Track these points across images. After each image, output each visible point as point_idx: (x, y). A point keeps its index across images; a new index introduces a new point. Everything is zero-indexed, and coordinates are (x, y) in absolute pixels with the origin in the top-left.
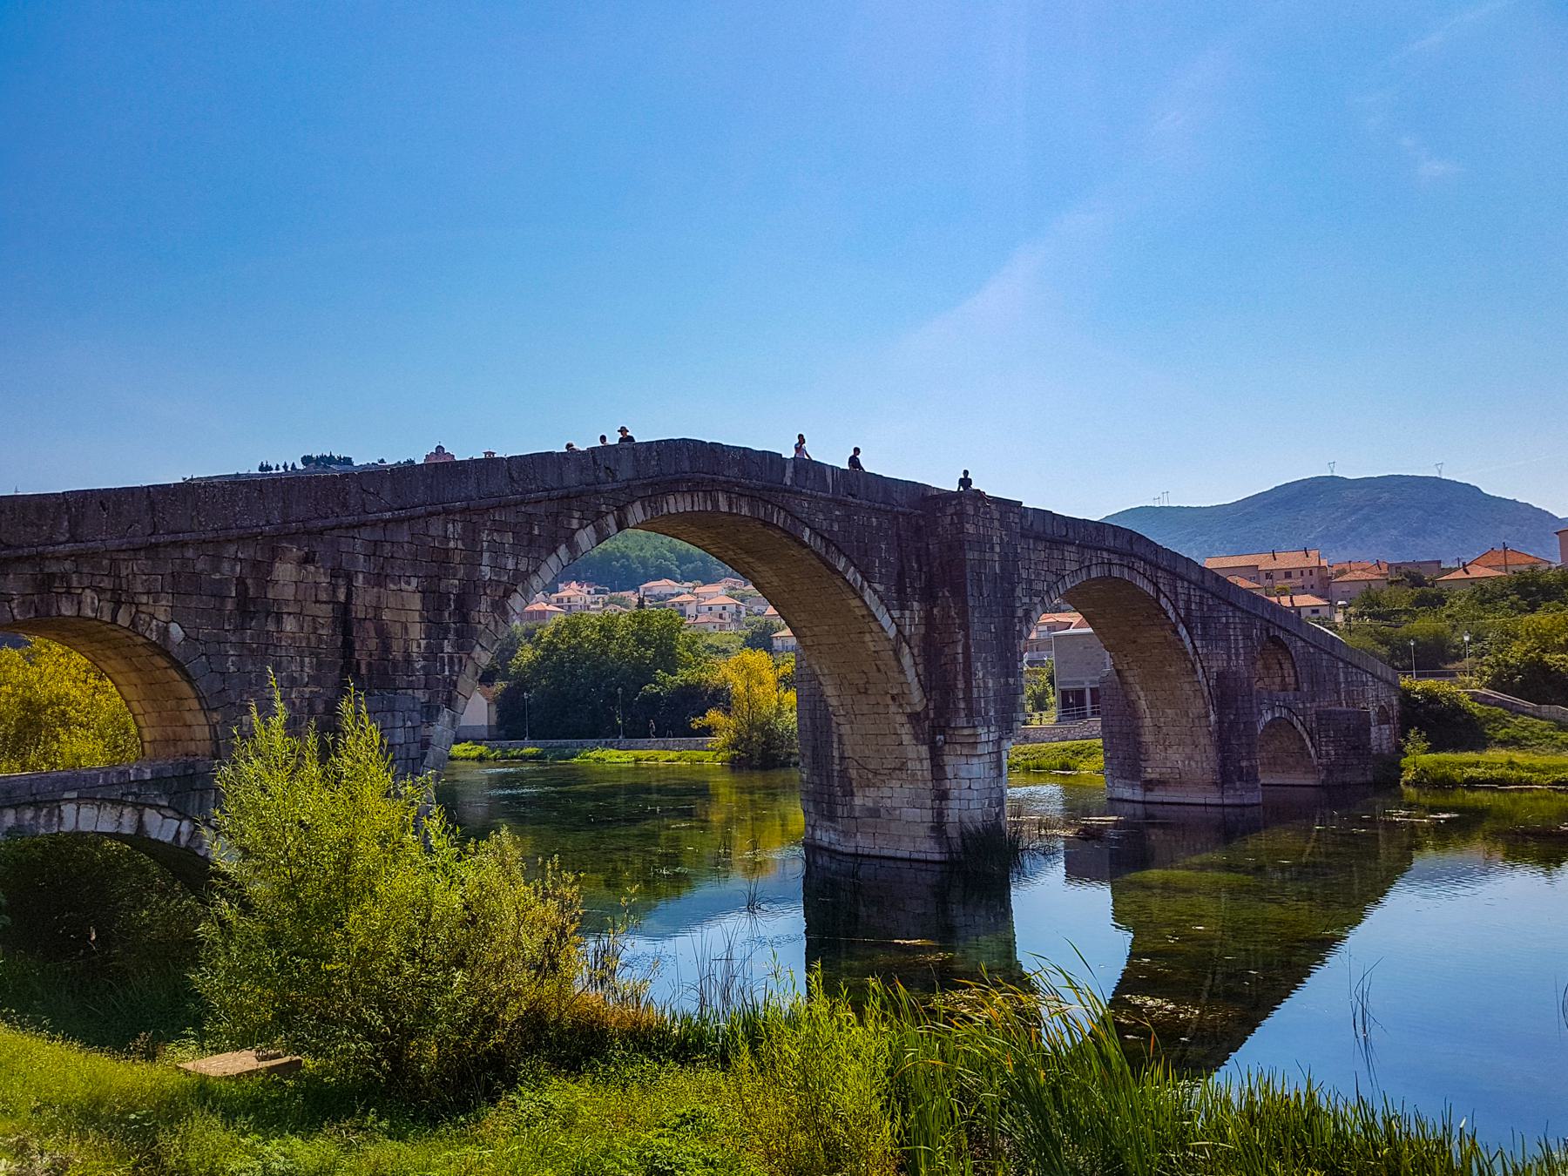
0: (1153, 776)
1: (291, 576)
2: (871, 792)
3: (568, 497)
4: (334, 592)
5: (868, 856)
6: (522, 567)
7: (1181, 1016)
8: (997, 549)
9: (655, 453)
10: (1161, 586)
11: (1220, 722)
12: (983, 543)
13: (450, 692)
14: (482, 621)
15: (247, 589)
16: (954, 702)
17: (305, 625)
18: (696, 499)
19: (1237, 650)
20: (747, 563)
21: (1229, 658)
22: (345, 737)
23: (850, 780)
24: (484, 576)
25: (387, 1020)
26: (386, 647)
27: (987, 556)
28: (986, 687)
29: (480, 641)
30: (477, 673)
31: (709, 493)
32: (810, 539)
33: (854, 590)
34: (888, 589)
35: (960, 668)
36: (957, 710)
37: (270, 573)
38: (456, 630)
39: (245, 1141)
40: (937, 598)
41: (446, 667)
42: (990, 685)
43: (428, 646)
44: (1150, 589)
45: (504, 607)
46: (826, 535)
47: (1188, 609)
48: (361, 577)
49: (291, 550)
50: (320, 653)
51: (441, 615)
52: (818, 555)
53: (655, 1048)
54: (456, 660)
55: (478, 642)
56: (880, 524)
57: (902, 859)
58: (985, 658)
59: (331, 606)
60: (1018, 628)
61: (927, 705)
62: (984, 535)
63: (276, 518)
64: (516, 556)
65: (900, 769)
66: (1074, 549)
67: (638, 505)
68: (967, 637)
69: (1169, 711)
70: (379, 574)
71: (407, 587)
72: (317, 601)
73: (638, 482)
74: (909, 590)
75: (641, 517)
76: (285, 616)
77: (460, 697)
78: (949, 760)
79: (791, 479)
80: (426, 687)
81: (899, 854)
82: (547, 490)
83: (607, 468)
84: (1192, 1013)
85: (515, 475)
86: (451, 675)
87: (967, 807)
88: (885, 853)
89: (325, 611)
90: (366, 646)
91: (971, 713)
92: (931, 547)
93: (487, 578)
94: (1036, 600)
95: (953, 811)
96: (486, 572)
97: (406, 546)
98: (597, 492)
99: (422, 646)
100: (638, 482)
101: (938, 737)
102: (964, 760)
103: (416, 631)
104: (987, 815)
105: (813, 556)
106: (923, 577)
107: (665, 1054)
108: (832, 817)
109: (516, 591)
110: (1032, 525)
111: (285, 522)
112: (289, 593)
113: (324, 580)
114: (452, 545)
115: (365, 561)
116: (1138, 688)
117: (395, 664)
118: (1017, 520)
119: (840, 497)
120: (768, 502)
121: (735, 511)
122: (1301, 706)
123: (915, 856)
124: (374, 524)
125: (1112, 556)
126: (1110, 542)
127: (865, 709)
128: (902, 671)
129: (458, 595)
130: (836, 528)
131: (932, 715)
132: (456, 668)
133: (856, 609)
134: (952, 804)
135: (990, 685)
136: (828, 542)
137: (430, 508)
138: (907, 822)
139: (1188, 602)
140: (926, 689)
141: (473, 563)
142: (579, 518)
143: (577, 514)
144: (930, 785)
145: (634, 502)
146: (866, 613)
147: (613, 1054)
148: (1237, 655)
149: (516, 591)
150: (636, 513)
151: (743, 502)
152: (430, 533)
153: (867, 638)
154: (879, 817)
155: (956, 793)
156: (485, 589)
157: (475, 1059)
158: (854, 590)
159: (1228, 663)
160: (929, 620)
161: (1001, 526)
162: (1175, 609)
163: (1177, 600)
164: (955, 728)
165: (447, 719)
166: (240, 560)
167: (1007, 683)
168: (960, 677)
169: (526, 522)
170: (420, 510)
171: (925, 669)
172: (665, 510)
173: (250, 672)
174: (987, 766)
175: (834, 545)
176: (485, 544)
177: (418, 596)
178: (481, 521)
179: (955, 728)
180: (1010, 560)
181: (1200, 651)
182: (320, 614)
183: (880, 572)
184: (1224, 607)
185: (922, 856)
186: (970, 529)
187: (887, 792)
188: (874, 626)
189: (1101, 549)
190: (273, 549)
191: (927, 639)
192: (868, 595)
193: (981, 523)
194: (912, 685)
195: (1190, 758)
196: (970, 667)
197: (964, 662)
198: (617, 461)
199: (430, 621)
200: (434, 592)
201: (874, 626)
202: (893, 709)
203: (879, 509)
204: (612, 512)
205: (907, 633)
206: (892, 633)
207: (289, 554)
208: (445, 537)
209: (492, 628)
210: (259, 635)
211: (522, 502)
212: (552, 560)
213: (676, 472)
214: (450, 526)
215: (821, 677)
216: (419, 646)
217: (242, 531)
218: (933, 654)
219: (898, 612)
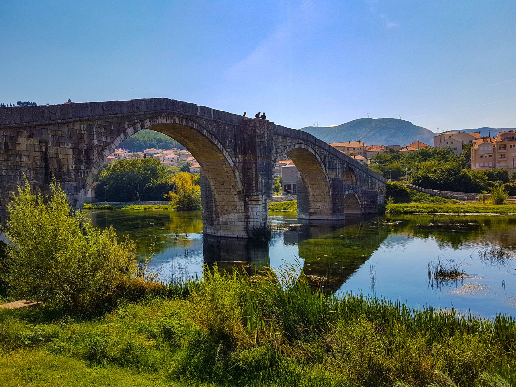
0: (312, 211)
1: (25, 142)
2: (225, 216)
3: (124, 117)
4: (41, 147)
5: (224, 237)
6: (108, 141)
7: (322, 280)
9: (153, 103)
10: (317, 151)
11: (333, 194)
12: (262, 136)
13: (84, 183)
14: (95, 159)
15: (8, 146)
16: (252, 188)
17: (31, 159)
18: (168, 119)
19: (339, 172)
20: (185, 141)
21: (336, 174)
22: (53, 195)
23: (218, 213)
24: (95, 143)
25: (71, 288)
27: (263, 140)
28: (262, 183)
29: (94, 166)
30: (93, 177)
31: (172, 117)
32: (206, 134)
33: (220, 151)
34: (231, 151)
35: (254, 176)
36: (253, 190)
37: (17, 141)
38: (85, 162)
39: (28, 326)
40: (247, 154)
41: (82, 175)
42: (263, 182)
43: (76, 167)
44: (313, 152)
45: (102, 154)
46: (211, 132)
47: (325, 159)
48: (50, 142)
49: (24, 133)
50: (37, 169)
51: (80, 157)
52: (208, 139)
53: (161, 294)
54: (86, 172)
55: (93, 166)
56: (229, 129)
57: (235, 238)
58: (262, 173)
59: (40, 153)
60: (272, 164)
61: (243, 189)
62: (262, 133)
63: (18, 121)
64: (106, 137)
65: (234, 209)
66: (290, 138)
67: (148, 121)
68: (256, 166)
69: (318, 191)
70: (57, 142)
71: (67, 147)
72: (35, 151)
73: (148, 112)
74: (238, 151)
75: (149, 125)
76: (23, 156)
77: (87, 185)
78: (250, 206)
79: (200, 113)
80: (75, 181)
81: (234, 236)
82: (115, 114)
83: (137, 107)
84: (325, 279)
85: (105, 108)
86: (84, 177)
87: (255, 221)
88: (230, 236)
89: (38, 155)
90: (53, 167)
91: (257, 191)
92: (245, 137)
93: (96, 144)
94: (278, 155)
95: (251, 222)
96: (95, 142)
97: (66, 132)
98: (134, 115)
99: (74, 167)
100: (148, 112)
101: (247, 199)
102: (255, 206)
103: (71, 162)
104: (262, 223)
105: (207, 139)
106: (242, 147)
107: (164, 296)
108: (212, 225)
109: (106, 149)
110: (277, 130)
111: (21, 123)
112: (24, 147)
113: (37, 144)
114: (83, 132)
115: (52, 137)
116: (308, 184)
117: (64, 174)
118: (273, 129)
119: (216, 120)
120: (193, 121)
121: (181, 123)
122: (357, 189)
123: (239, 236)
124: (55, 124)
125: (302, 141)
126: (301, 137)
127: (223, 190)
128: (235, 178)
129: (86, 150)
130: (214, 130)
131: (245, 192)
132: (86, 175)
133: (221, 157)
134: (251, 220)
135: (263, 182)
136: (212, 135)
137: (74, 119)
138: (237, 226)
139: (325, 156)
140: (243, 183)
141: (91, 139)
142: (128, 124)
143: (127, 123)
144: (244, 214)
145: (147, 119)
146: (224, 158)
147: (147, 296)
148: (339, 173)
149: (106, 149)
150: (148, 123)
151: (184, 120)
152: (75, 128)
153: (224, 166)
154: (228, 224)
155: (252, 216)
156: (95, 148)
157: (102, 299)
158: (220, 151)
159: (336, 176)
160: (244, 161)
162: (321, 159)
163: (321, 156)
164: (252, 196)
165: (83, 192)
166: (5, 136)
167: (269, 181)
168: (254, 180)
169: (109, 125)
170: (71, 120)
171: (243, 177)
172: (157, 122)
173: (11, 176)
174: (262, 208)
175: (214, 136)
176: (95, 132)
177: (71, 150)
178: (93, 124)
179: (252, 196)
180: (270, 142)
181: (328, 172)
182: (36, 155)
183: (229, 145)
185: (241, 236)
186: (258, 131)
187: (230, 216)
188: (226, 162)
190: (18, 132)
191: (243, 167)
192: (225, 152)
193: (261, 129)
194: (238, 182)
195: (324, 206)
196: (257, 176)
197: (255, 174)
198: (141, 105)
199: (76, 159)
200: (77, 149)
201: (226, 162)
202: (232, 190)
203: (228, 124)
204: (139, 122)
205: (237, 165)
206: (232, 165)
207: (23, 134)
208: (81, 129)
209: (98, 161)
210: (13, 163)
211: (107, 118)
212: (119, 139)
213: (161, 110)
214: (82, 126)
215: (209, 180)
216: (72, 167)
217: (5, 125)
218: (245, 171)
219: (234, 158)
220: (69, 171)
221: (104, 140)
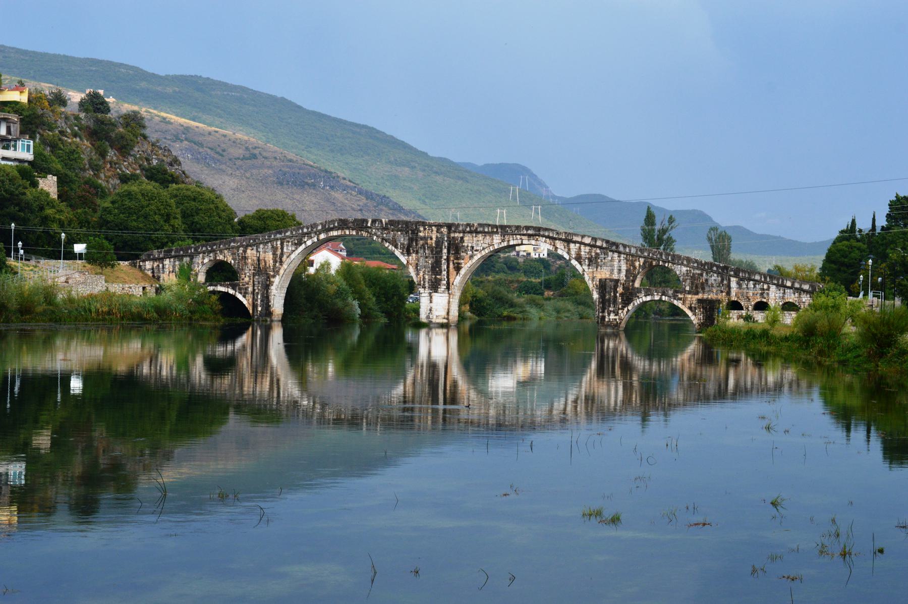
8: (434, 239)
10: (558, 246)
21: (612, 272)
26: (266, 264)
28: (424, 278)
34: (403, 251)
94: (475, 253)
103: (271, 262)
110: (476, 229)
125: (523, 237)
136: (383, 239)
141: (282, 249)
161: (437, 232)
162: (569, 253)
167: (436, 277)
181: (586, 270)
184: (610, 254)
189: (516, 235)
220: (270, 266)
221: (290, 249)
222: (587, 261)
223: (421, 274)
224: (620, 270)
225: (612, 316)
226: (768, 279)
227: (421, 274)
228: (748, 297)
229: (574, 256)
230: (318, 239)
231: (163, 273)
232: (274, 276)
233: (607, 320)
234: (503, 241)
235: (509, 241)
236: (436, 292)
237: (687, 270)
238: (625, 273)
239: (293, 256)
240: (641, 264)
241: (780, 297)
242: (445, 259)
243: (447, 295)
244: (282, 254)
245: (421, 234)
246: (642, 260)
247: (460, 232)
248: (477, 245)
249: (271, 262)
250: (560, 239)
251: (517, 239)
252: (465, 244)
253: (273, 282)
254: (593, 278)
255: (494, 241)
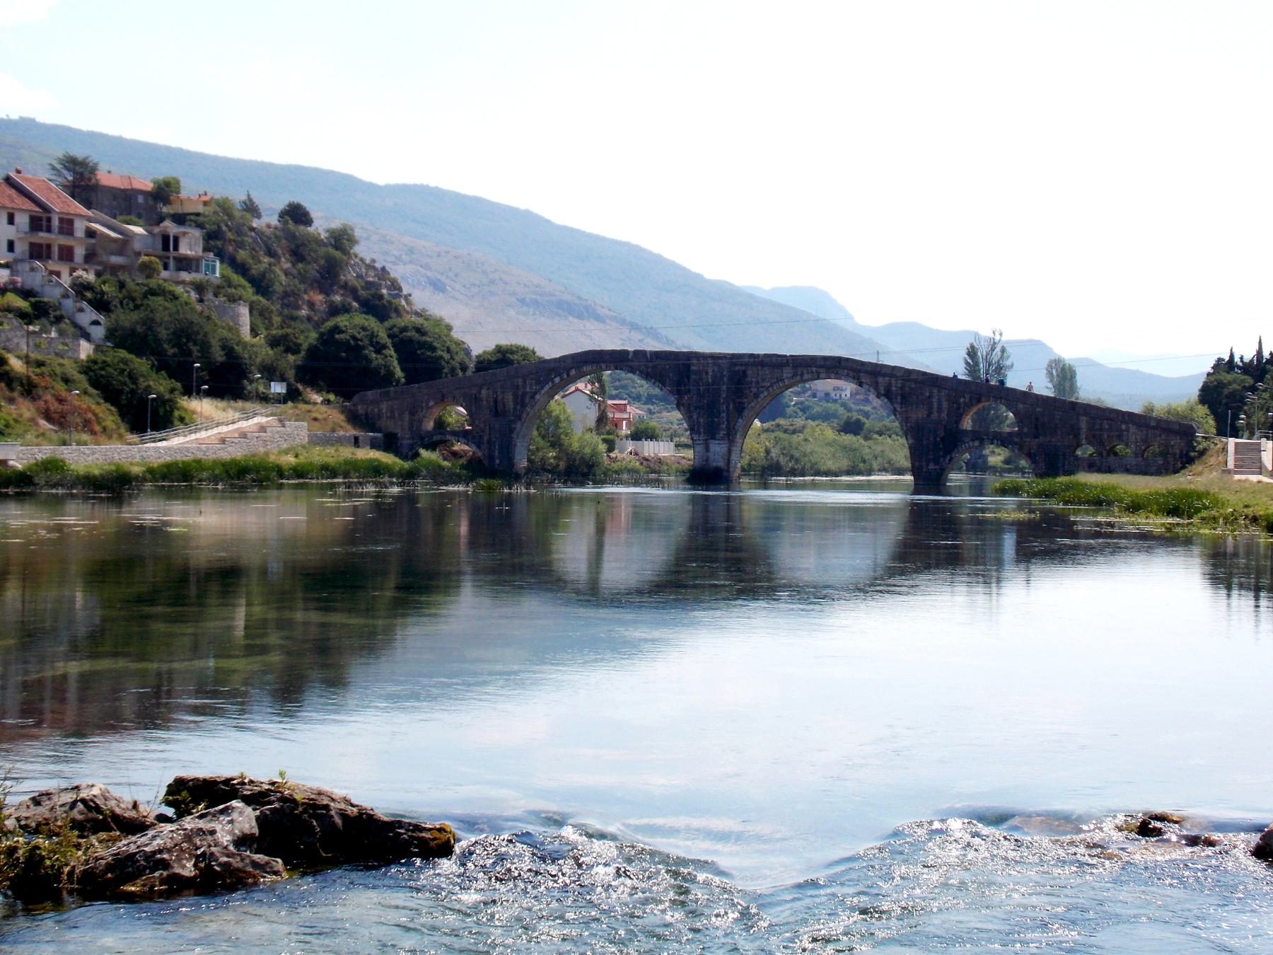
8: (710, 374)
10: (863, 380)
26: (504, 407)
28: (698, 422)
67: (574, 370)
89: (491, 400)
90: (500, 408)
122: (1016, 440)
141: (525, 387)
159: (928, 416)
181: (899, 409)
189: (810, 367)
222: (899, 397)
223: (695, 417)
224: (940, 410)
225: (931, 466)
226: (1127, 418)
227: (695, 417)
228: (1101, 441)
229: (882, 392)
230: (568, 375)
231: (380, 417)
232: (514, 422)
233: (924, 470)
234: (795, 375)
235: (802, 375)
236: (714, 438)
237: (1024, 408)
238: (946, 413)
239: (537, 397)
240: (967, 400)
241: (1142, 441)
242: (724, 398)
243: (727, 442)
244: (524, 394)
245: (694, 368)
246: (967, 396)
247: (742, 365)
248: (764, 380)
249: (511, 405)
250: (866, 372)
251: (812, 372)
252: (749, 379)
253: (514, 429)
254: (907, 419)
255: (785, 375)
